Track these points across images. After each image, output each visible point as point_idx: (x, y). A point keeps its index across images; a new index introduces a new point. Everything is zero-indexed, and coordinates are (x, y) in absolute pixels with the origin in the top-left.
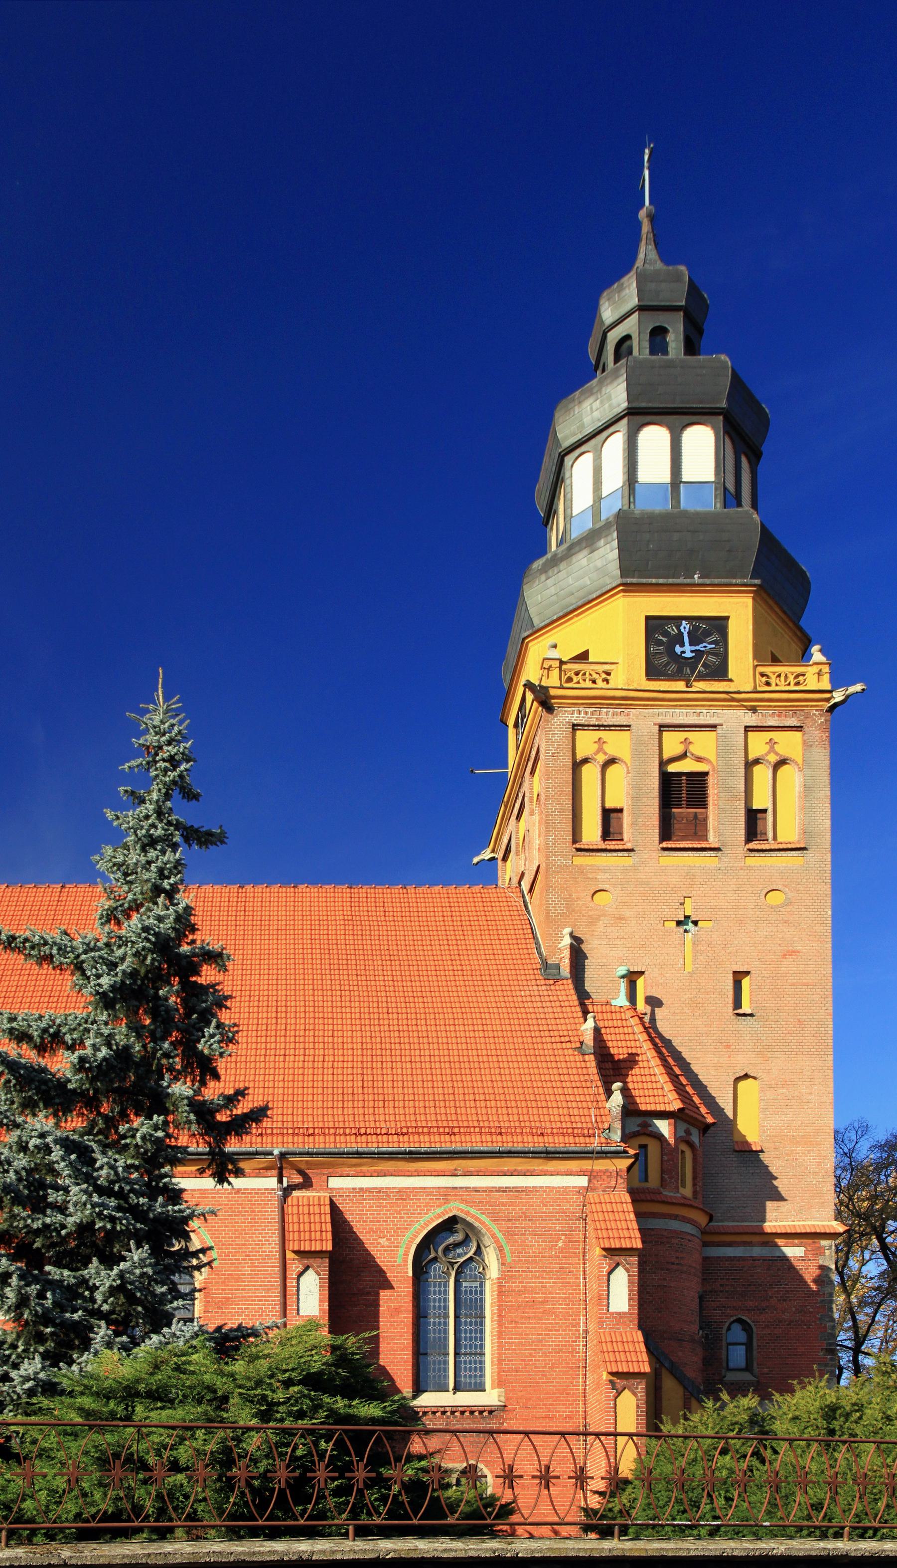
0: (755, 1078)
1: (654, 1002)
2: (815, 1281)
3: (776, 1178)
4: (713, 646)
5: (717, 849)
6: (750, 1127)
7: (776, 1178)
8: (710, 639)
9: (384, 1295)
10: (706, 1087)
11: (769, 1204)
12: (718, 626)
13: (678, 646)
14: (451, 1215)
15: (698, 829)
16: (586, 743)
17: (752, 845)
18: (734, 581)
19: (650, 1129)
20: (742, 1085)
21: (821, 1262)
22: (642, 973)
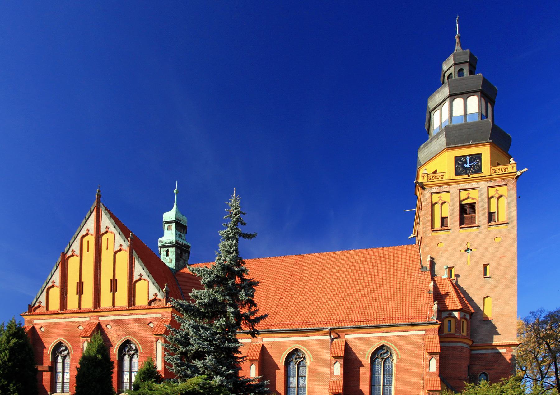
5: (479, 226)
9: (361, 369)
11: (495, 337)
12: (479, 157)
15: (473, 221)
17: (490, 224)
20: (486, 299)
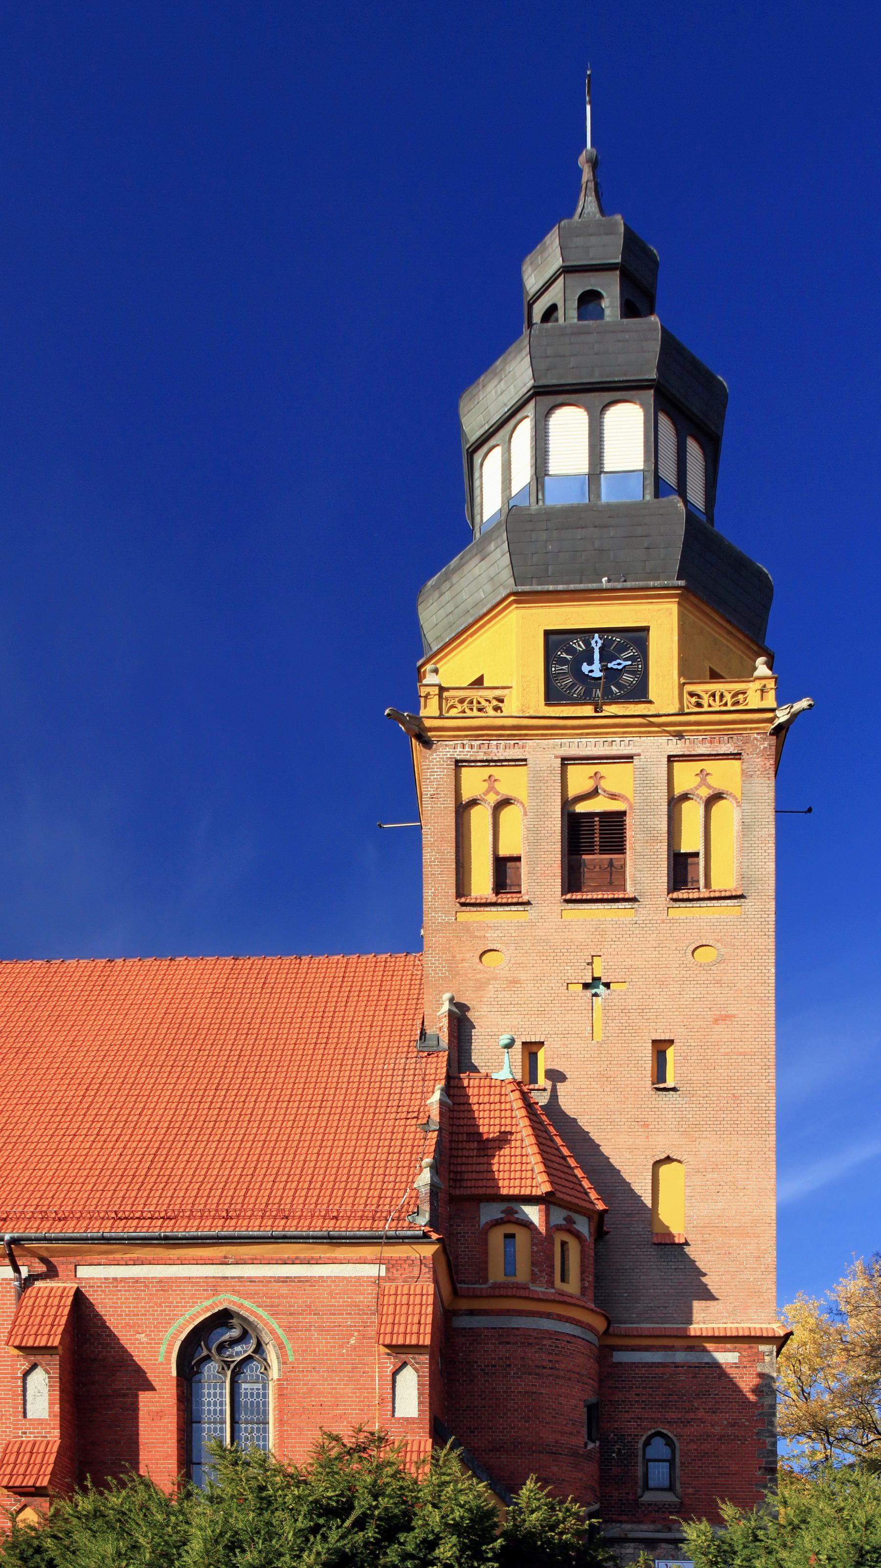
0: (680, 1162)
1: (556, 1076)
3: (705, 1275)
4: (630, 663)
6: (674, 1216)
7: (705, 1275)
8: (625, 655)
10: (619, 1171)
11: (697, 1305)
12: (637, 638)
13: (585, 664)
14: (221, 1308)
15: (614, 877)
16: (473, 782)
18: (651, 584)
19: (516, 1216)
20: (664, 1170)
21: (759, 1370)
22: (541, 1044)
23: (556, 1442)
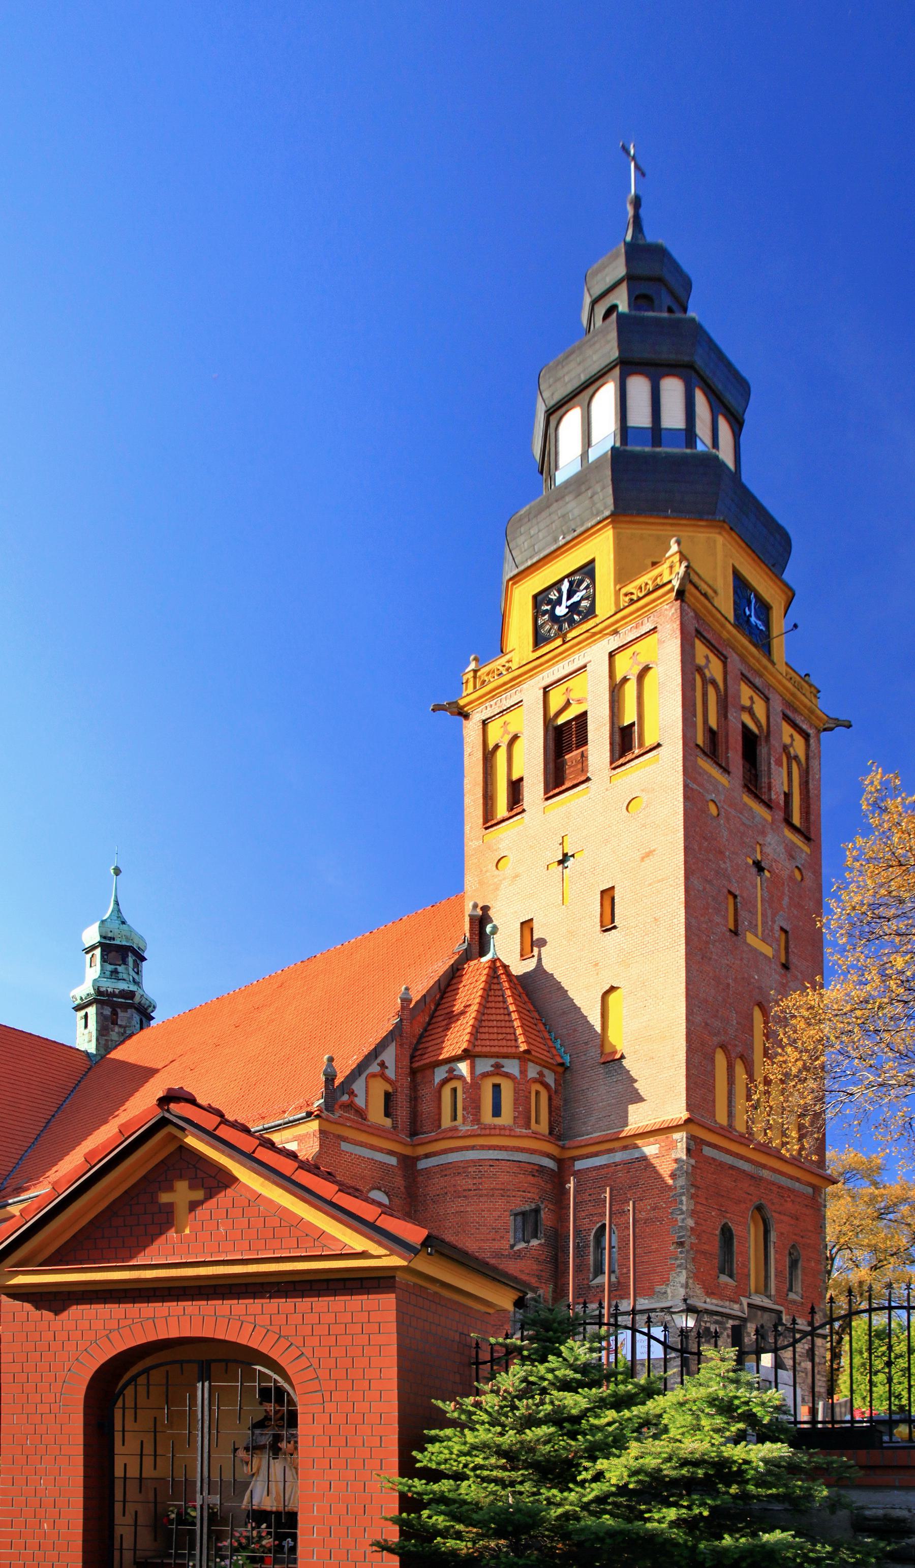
2: (673, 1176)
23: (480, 1248)
